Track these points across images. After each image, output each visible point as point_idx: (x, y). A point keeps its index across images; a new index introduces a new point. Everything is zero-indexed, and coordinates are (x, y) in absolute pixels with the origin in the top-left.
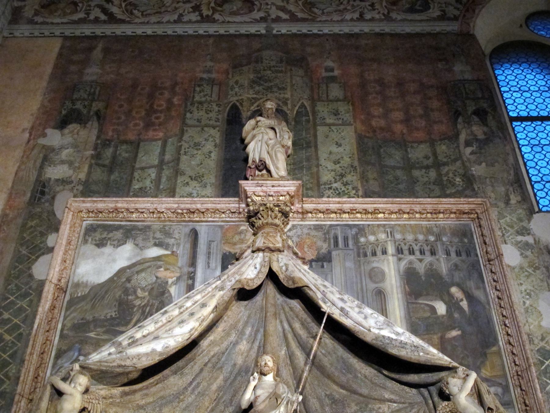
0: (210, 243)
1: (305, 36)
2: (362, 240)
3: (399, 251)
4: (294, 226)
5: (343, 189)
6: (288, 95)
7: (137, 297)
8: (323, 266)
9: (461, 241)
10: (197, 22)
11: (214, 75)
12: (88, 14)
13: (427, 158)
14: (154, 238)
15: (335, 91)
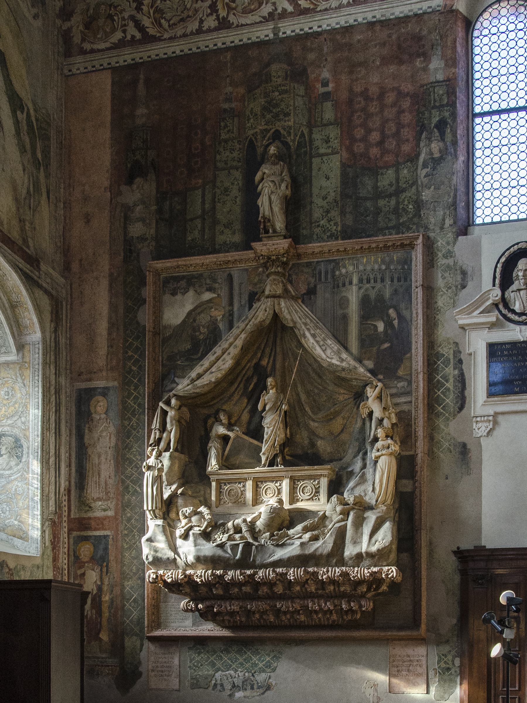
0: (240, 284)
1: (307, 36)
2: (337, 273)
3: (361, 281)
4: (293, 264)
5: (328, 226)
6: (291, 123)
7: (201, 333)
8: (310, 299)
9: (403, 268)
10: (216, 29)
11: (233, 105)
12: (124, 31)
13: (391, 185)
14: (206, 284)
15: (328, 112)
